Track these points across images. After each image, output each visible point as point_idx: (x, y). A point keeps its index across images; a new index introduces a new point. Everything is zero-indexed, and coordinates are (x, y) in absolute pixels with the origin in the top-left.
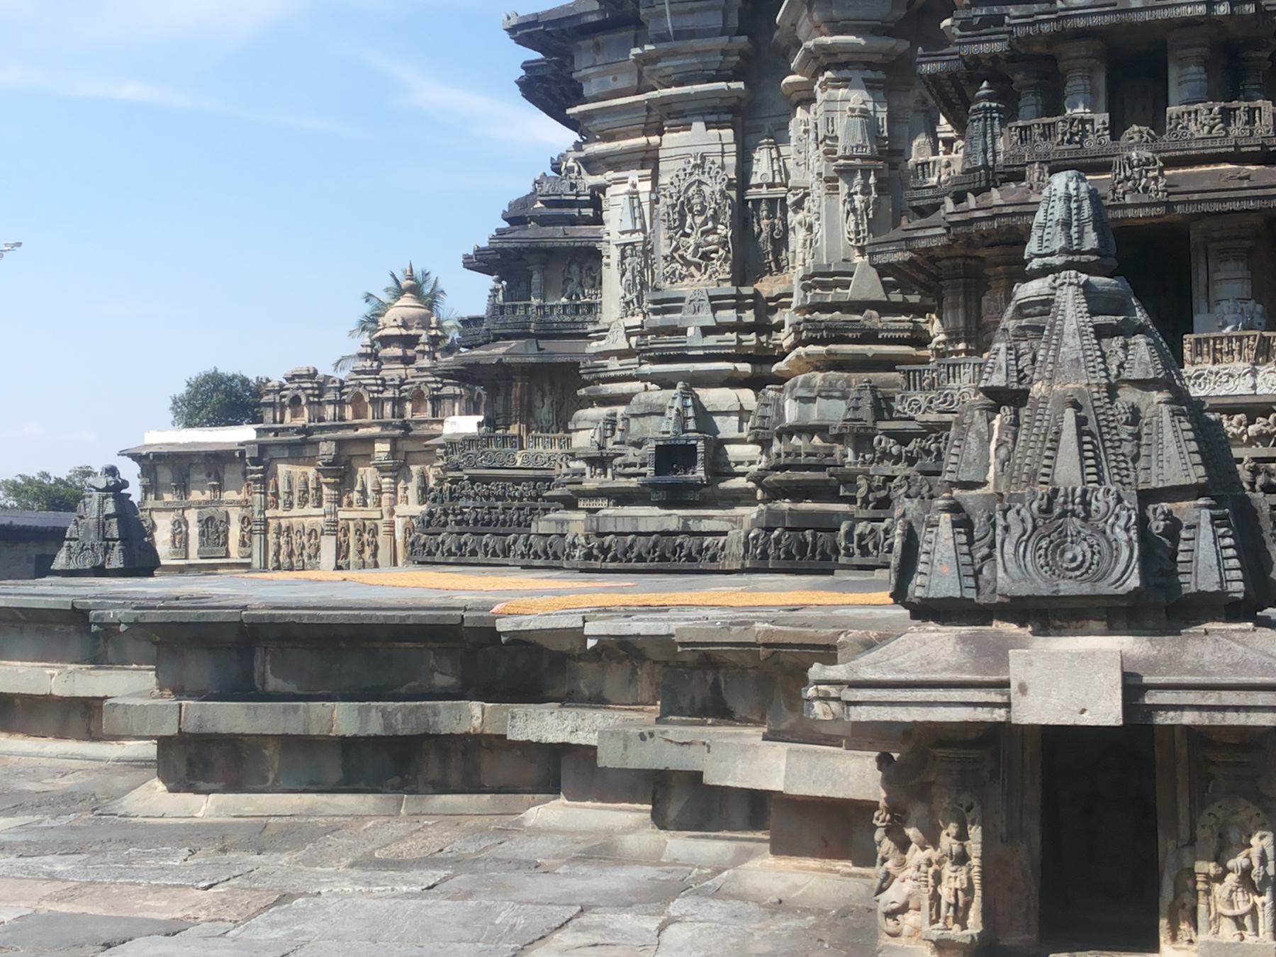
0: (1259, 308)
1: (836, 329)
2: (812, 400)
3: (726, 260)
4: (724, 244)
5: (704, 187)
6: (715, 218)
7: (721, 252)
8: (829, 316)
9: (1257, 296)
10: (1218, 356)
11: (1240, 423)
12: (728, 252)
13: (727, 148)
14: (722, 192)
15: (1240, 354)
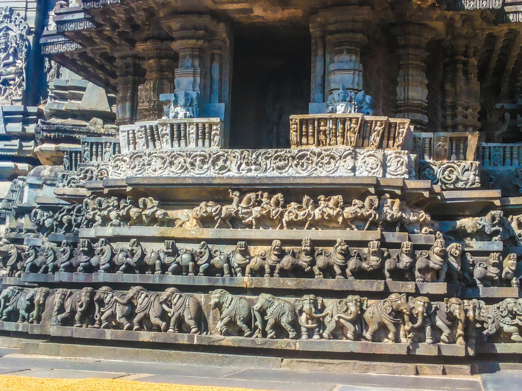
0: (368, 98)
1: (65, 131)
2: (40, 187)
3: (20, 86)
4: (20, 74)
5: (10, 32)
6: (15, 54)
7: (17, 80)
8: (63, 121)
9: (367, 88)
10: (322, 137)
11: (337, 205)
12: (23, 80)
13: (30, 5)
14: (21, 36)
15: (343, 136)
